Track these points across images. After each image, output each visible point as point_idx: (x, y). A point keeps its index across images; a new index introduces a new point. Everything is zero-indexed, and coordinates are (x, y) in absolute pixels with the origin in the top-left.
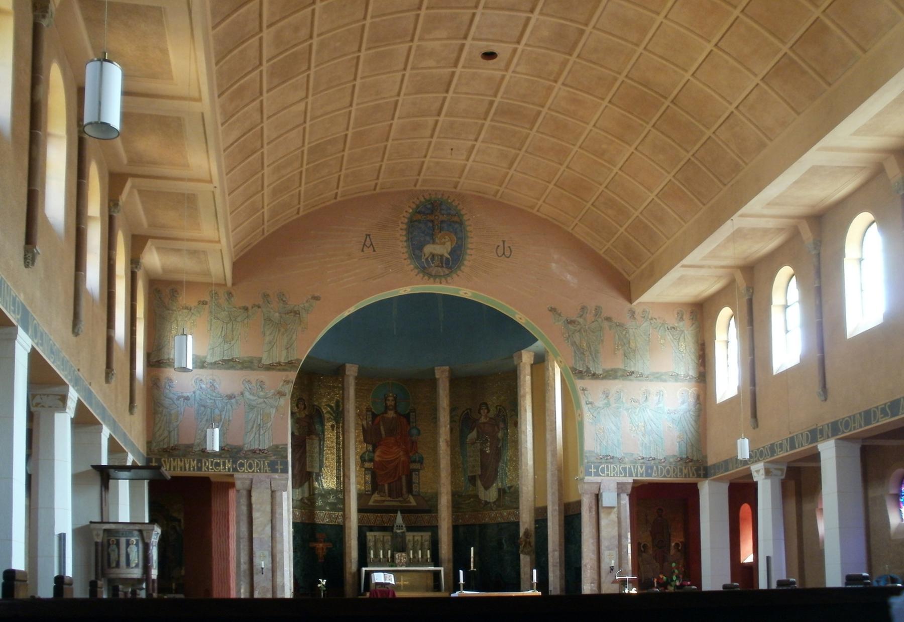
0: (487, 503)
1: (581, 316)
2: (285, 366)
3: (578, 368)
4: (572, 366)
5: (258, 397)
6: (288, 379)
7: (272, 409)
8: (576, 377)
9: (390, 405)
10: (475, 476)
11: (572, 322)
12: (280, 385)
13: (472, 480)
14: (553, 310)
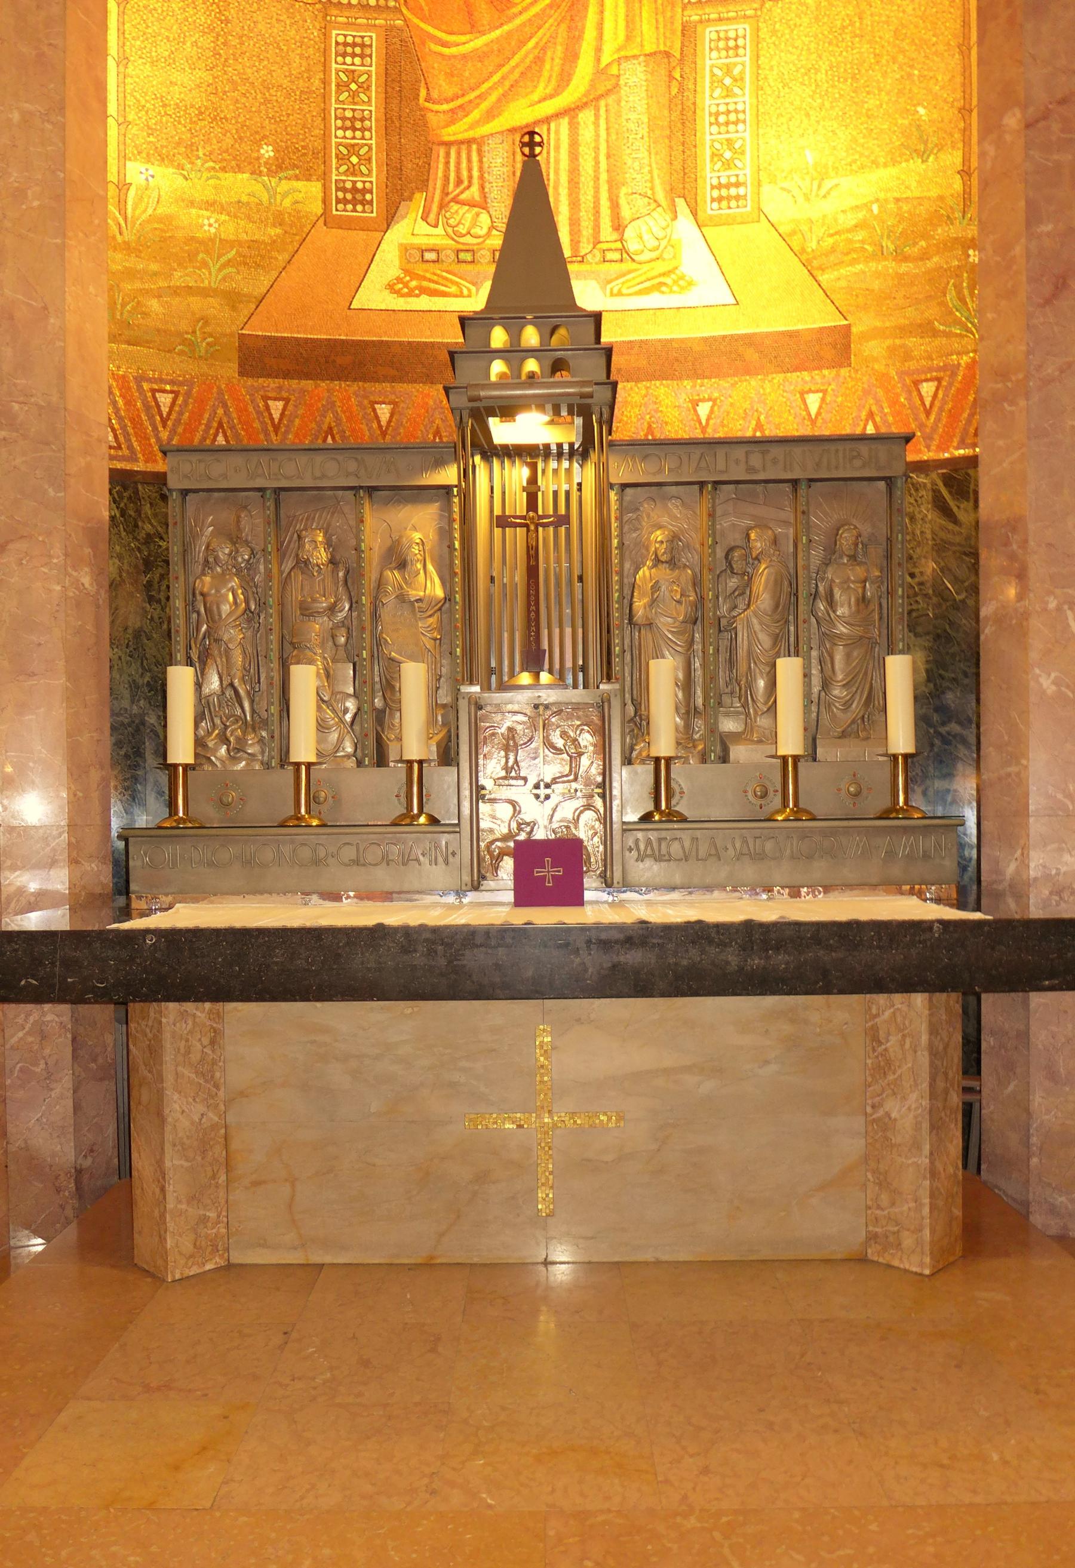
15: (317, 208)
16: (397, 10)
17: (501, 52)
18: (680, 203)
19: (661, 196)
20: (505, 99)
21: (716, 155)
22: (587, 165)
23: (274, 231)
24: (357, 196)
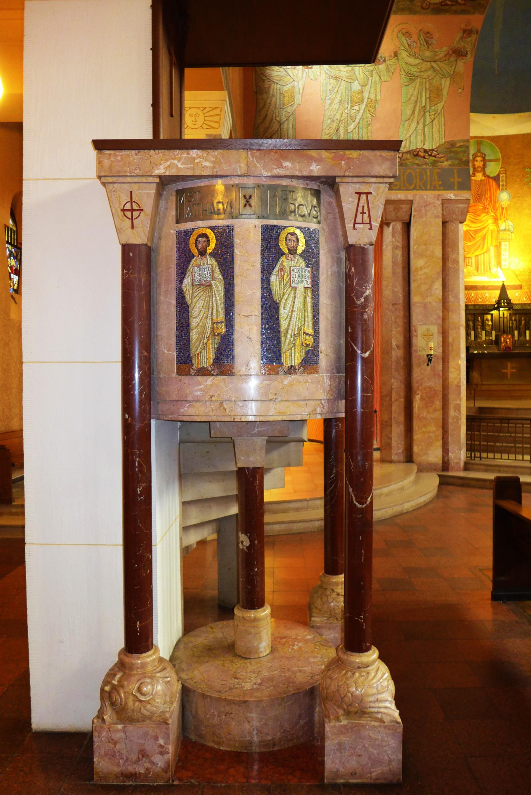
2: (464, 4)
5: (422, 59)
6: (470, 27)
7: (444, 80)
9: (479, 167)
12: (457, 39)
17: (474, 245)
18: (499, 266)
19: (496, 265)
20: (475, 251)
22: (485, 260)
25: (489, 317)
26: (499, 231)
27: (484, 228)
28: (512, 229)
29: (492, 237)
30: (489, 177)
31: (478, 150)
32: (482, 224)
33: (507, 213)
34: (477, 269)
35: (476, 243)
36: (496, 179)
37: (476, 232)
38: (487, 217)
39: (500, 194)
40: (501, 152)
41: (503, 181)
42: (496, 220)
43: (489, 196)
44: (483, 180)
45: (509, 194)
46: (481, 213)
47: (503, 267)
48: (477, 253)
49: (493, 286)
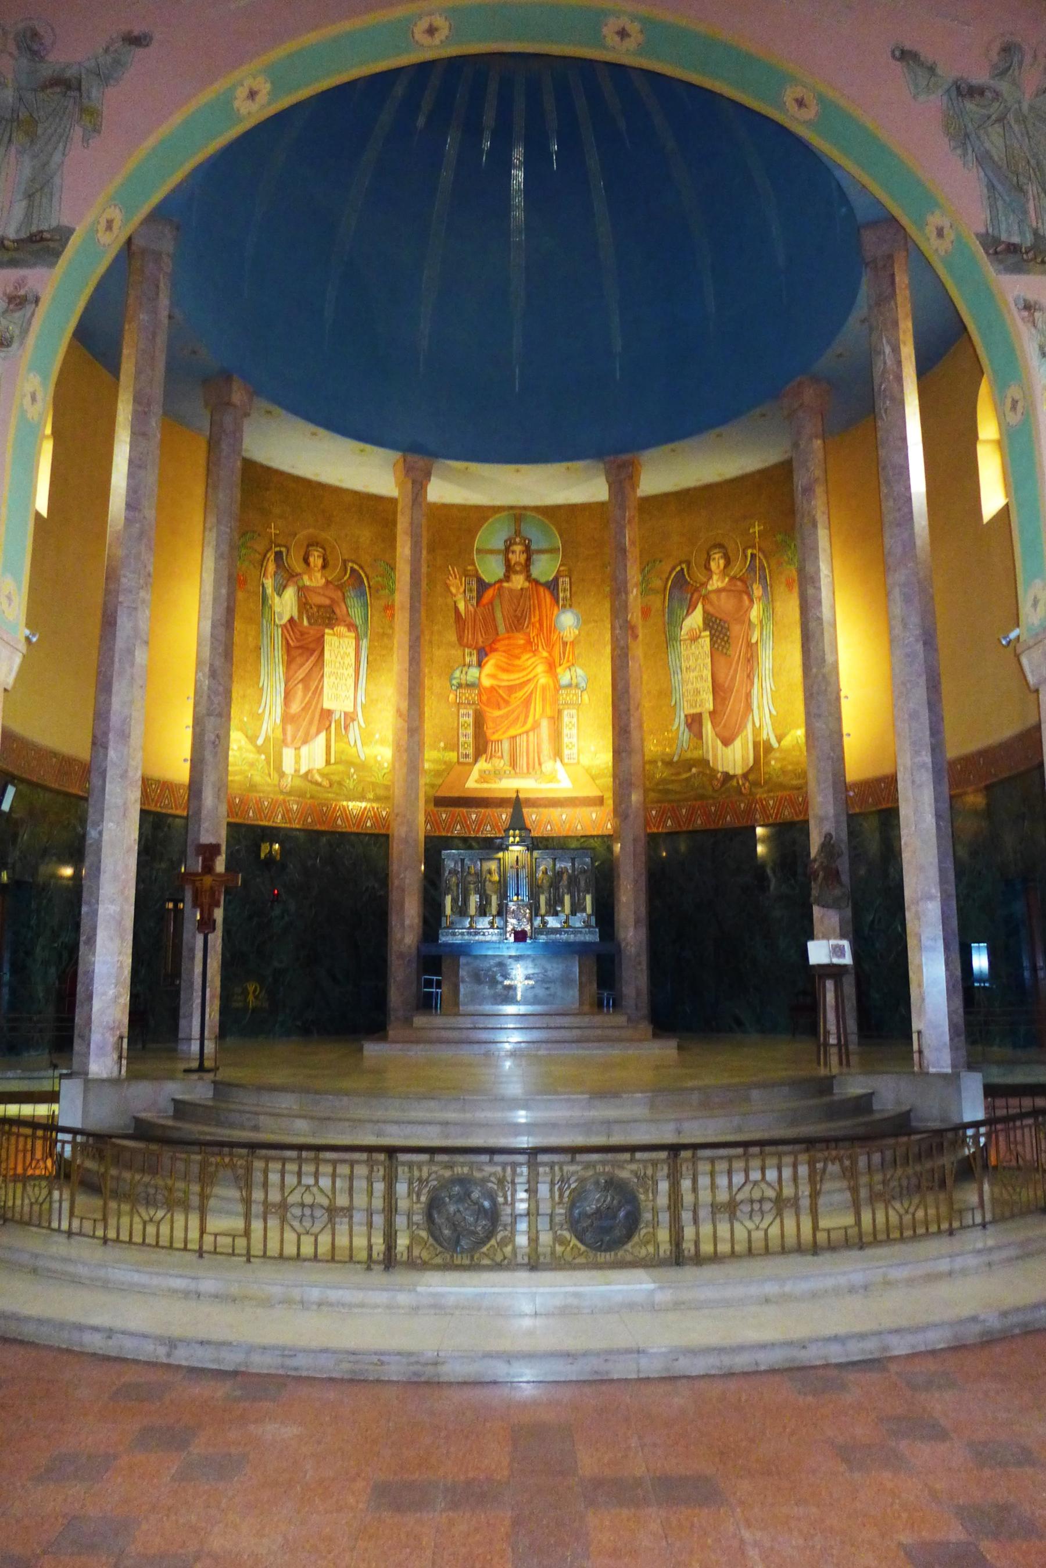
0: (727, 777)
1: (1002, 74)
2: (16, 249)
3: (1004, 237)
4: (983, 230)
6: (22, 292)
8: (1001, 267)
10: (700, 715)
11: (974, 92)
13: (694, 722)
14: (905, 55)
15: (455, 760)
16: (478, 704)
17: (506, 716)
18: (558, 759)
20: (508, 728)
21: (567, 746)
23: (444, 767)
24: (467, 756)
25: (493, 866)
26: (558, 688)
27: (529, 681)
28: (583, 685)
29: (544, 700)
30: (537, 582)
31: (515, 532)
32: (525, 673)
33: (573, 653)
34: (513, 764)
35: (513, 711)
36: (552, 586)
37: (511, 689)
38: (533, 660)
39: (558, 616)
40: (561, 536)
41: (565, 590)
42: (551, 667)
43: (537, 618)
44: (527, 589)
45: (577, 616)
46: (522, 653)
47: (566, 761)
48: (512, 732)
49: (547, 799)
